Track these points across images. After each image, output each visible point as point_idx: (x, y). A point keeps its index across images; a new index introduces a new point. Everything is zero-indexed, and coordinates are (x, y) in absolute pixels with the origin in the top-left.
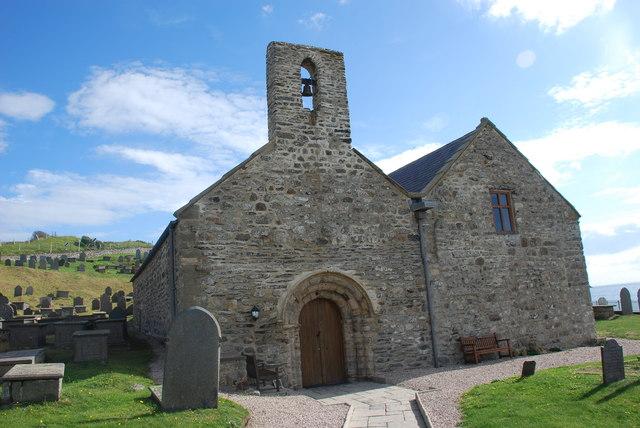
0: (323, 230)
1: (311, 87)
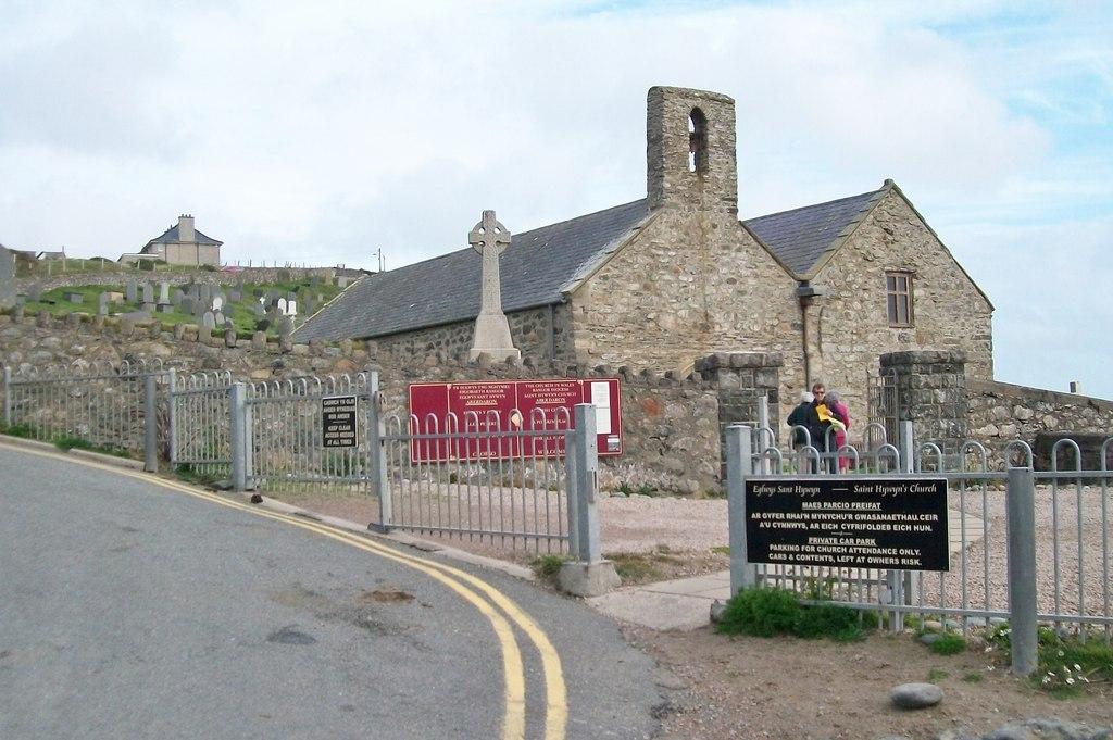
0: (707, 315)
1: (699, 141)
